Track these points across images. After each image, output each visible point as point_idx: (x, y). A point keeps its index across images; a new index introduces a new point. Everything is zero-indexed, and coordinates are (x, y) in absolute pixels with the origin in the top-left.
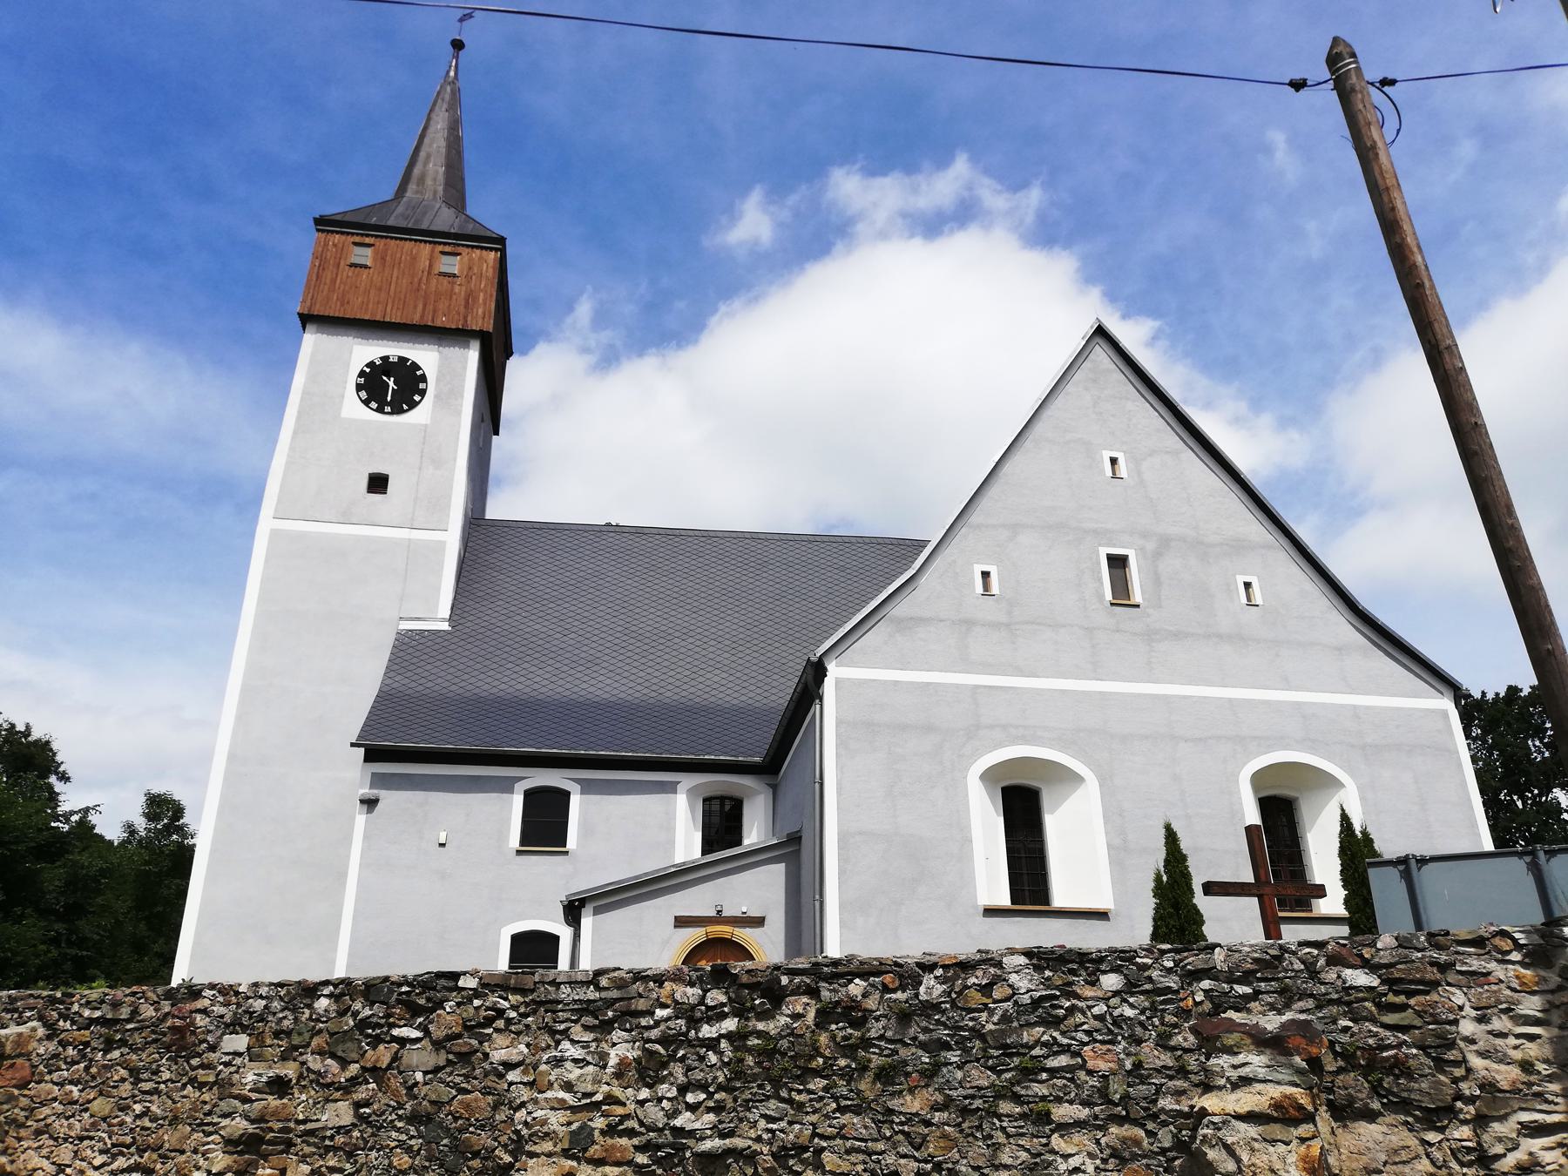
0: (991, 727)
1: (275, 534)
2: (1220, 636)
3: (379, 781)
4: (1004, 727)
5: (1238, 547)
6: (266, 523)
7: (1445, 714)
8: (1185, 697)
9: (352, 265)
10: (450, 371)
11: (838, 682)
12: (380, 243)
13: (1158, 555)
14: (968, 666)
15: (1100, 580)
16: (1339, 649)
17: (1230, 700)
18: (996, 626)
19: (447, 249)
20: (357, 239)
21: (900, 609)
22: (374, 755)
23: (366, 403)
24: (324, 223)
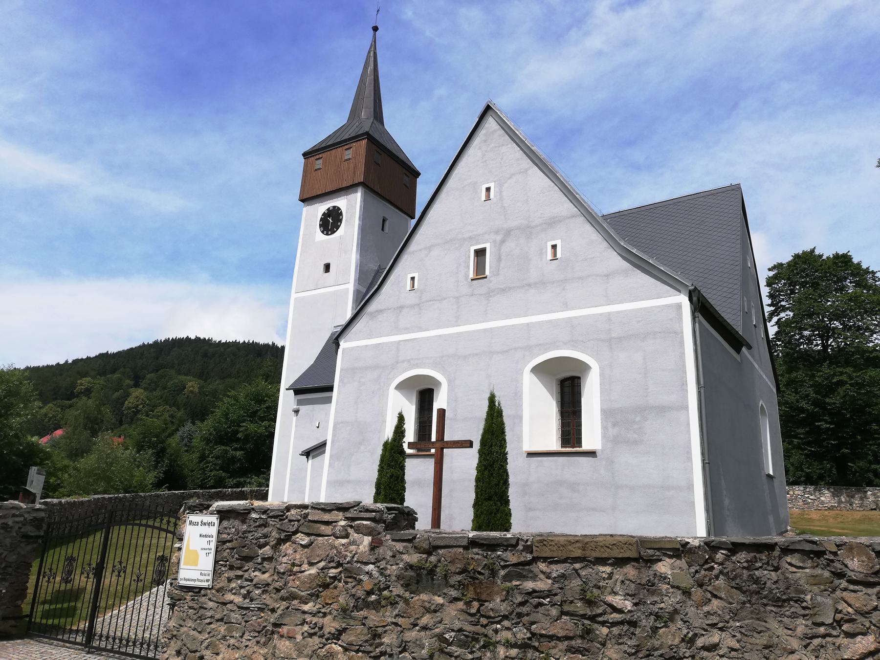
0: (403, 361)
1: (296, 299)
2: (529, 285)
3: (300, 403)
4: (409, 361)
5: (552, 223)
6: (294, 296)
7: (679, 306)
8: (502, 327)
10: (351, 205)
11: (344, 349)
12: (324, 155)
13: (503, 241)
14: (398, 330)
15: (468, 267)
16: (607, 276)
18: (412, 306)
19: (347, 147)
20: (317, 157)
22: (297, 392)
23: (323, 232)
24: (306, 155)
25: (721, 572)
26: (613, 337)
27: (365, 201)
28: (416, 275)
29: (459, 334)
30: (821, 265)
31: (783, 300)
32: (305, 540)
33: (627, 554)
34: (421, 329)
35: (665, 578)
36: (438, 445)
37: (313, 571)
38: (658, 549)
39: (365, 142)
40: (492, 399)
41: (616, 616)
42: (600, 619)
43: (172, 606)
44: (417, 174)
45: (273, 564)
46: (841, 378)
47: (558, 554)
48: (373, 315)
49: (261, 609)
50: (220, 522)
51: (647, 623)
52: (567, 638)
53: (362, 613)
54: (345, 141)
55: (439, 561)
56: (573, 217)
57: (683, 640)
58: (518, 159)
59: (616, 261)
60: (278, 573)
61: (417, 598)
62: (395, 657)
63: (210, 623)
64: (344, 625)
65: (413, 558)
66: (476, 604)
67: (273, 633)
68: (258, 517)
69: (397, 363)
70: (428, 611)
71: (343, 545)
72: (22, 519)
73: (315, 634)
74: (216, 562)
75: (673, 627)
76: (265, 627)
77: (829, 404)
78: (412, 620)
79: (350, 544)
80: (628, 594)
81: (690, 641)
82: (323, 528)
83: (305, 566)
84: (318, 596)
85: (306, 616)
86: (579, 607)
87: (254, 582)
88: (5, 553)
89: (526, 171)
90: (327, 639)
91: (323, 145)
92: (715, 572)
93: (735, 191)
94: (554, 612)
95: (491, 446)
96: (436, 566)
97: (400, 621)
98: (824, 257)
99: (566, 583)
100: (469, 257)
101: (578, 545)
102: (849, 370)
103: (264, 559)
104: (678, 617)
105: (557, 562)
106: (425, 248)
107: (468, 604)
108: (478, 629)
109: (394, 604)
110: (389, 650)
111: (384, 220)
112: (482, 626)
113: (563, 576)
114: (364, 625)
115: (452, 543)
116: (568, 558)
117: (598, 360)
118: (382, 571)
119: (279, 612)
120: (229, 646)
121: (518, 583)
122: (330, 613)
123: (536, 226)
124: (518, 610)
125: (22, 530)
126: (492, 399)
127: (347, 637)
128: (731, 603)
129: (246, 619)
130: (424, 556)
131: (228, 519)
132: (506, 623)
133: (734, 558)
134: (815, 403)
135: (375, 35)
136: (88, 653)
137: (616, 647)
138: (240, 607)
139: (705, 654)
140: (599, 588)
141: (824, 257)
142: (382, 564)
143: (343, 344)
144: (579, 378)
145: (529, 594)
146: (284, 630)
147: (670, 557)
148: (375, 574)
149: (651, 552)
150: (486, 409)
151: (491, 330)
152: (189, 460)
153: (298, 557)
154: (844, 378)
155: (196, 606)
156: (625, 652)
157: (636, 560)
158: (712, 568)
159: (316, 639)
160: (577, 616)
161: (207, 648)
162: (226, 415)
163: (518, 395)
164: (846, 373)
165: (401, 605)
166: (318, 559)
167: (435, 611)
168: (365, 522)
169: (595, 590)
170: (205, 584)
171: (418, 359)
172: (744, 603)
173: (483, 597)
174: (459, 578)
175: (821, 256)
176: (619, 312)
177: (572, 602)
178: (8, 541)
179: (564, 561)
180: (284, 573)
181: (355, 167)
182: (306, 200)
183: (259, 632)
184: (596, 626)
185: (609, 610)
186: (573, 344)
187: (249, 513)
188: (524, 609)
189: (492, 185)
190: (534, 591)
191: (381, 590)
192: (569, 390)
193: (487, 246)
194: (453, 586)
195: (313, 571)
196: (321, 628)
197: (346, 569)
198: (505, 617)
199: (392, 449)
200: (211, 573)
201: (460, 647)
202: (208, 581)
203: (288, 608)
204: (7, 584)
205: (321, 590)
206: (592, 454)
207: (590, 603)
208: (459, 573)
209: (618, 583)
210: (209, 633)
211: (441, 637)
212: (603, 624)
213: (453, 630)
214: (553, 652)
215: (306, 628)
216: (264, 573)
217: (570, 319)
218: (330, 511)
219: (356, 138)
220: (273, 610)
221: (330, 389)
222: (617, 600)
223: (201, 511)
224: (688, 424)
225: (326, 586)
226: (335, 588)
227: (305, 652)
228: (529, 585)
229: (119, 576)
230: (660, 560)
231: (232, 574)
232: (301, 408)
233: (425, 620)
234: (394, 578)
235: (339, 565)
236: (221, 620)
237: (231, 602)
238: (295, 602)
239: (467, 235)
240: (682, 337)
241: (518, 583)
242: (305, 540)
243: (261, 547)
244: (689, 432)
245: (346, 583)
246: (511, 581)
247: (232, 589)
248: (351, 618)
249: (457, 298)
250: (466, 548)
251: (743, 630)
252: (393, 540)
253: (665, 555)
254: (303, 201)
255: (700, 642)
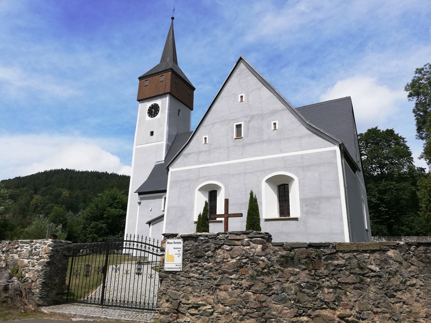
0: (202, 178)
2: (263, 141)
3: (141, 199)
4: (205, 177)
5: (273, 113)
6: (135, 147)
7: (335, 151)
8: (251, 161)
9: (146, 86)
10: (164, 103)
11: (171, 172)
13: (250, 121)
15: (233, 133)
16: (301, 137)
17: (263, 160)
18: (206, 151)
20: (146, 79)
21: (185, 152)
22: (140, 194)
23: (149, 116)
24: (140, 78)
25: (414, 255)
26: (304, 165)
27: (170, 101)
28: (207, 137)
29: (229, 164)
30: (381, 135)
31: (363, 151)
32: (228, 248)
33: (376, 248)
34: (211, 162)
35: (391, 257)
36: (226, 216)
37: (234, 261)
38: (388, 246)
39: (170, 73)
40: (251, 194)
41: (373, 274)
42: (367, 275)
43: (161, 281)
44: (194, 89)
45: (214, 259)
46: (390, 187)
47: (346, 249)
48: (186, 156)
49: (209, 279)
50: (184, 242)
51: (386, 276)
52: (354, 283)
53: (262, 277)
54: (160, 72)
55: (295, 254)
56: (283, 110)
57: (401, 283)
58: (256, 83)
59: (304, 130)
60: (216, 263)
61: (287, 269)
62: (280, 294)
63: (183, 287)
64: (252, 283)
65: (284, 253)
66: (313, 271)
67: (216, 289)
68: (203, 238)
69: (199, 178)
70: (293, 275)
71: (248, 249)
72: (63, 247)
73: (238, 288)
74: (183, 260)
75: (396, 278)
76: (212, 286)
77: (385, 199)
78: (286, 279)
79: (251, 248)
80: (377, 265)
81: (404, 283)
82: (236, 242)
83: (229, 259)
84: (237, 271)
85: (233, 280)
86: (357, 270)
87: (204, 267)
88: (57, 263)
89: (259, 89)
90: (244, 290)
91: (149, 74)
92: (411, 255)
93: (349, 99)
94: (347, 273)
95: (253, 216)
96: (294, 256)
97: (280, 279)
98: (381, 131)
99: (351, 261)
100: (233, 128)
101: (355, 245)
102: (394, 183)
103: (208, 257)
104: (398, 274)
105: (346, 253)
106: (211, 124)
107: (310, 271)
108: (315, 281)
109: (276, 272)
110: (276, 292)
111: (179, 111)
112: (317, 280)
113: (350, 258)
114: (263, 282)
115: (301, 246)
116: (351, 251)
117: (297, 176)
118: (269, 259)
119: (219, 279)
120: (194, 296)
121: (331, 262)
122: (245, 278)
123: (266, 114)
124: (332, 273)
125: (63, 253)
126: (251, 194)
127: (254, 288)
128: (419, 267)
129: (201, 283)
130: (288, 252)
131: (188, 240)
132: (327, 278)
133: (418, 249)
134: (378, 199)
135: (172, 21)
136: (103, 308)
137: (374, 286)
138: (197, 279)
139: (411, 288)
140: (365, 262)
141: (381, 131)
142: (269, 256)
143: (171, 169)
144: (288, 185)
145: (336, 266)
146: (222, 287)
147: (393, 249)
148: (266, 260)
149: (385, 247)
150: (249, 199)
151: (245, 162)
152: (78, 229)
153: (226, 255)
154: (392, 186)
155: (175, 280)
156: (378, 288)
157: (379, 250)
158: (410, 253)
159: (239, 290)
160: (356, 274)
161: (183, 298)
162: (97, 206)
163: (260, 192)
164: (393, 184)
165: (280, 273)
166: (236, 255)
167: (296, 275)
168: (258, 239)
169: (363, 263)
170: (179, 270)
171: (210, 176)
172: (424, 267)
173: (316, 268)
174: (305, 260)
175: (380, 130)
176: (307, 154)
177: (354, 269)
178: (58, 258)
179: (350, 252)
180: (219, 263)
181: (166, 85)
182: (141, 100)
183: (209, 289)
184: (364, 278)
185: (370, 271)
186: (285, 168)
187: (198, 237)
188: (334, 272)
189: (243, 95)
190: (338, 265)
191: (269, 267)
192: (283, 190)
193: (242, 123)
194: (303, 264)
195: (234, 261)
196: (241, 285)
197: (251, 259)
198: (327, 276)
199: (203, 218)
200: (181, 265)
201: (308, 289)
202: (180, 268)
203: (223, 277)
204: (58, 278)
205: (239, 268)
206: (296, 219)
207: (362, 268)
208: (305, 258)
209: (372, 260)
210: (183, 291)
211: (299, 285)
212: (368, 277)
213: (305, 282)
214: (348, 289)
215: (233, 285)
216: (209, 263)
217: (284, 157)
218: (239, 235)
219: (166, 71)
220: (215, 279)
221: (165, 191)
222: (373, 267)
223: (173, 238)
224: (341, 205)
225: (241, 267)
226: (246, 267)
227: (234, 296)
228: (336, 262)
229: (116, 272)
230: (389, 250)
231: (192, 264)
232: (142, 201)
233: (292, 278)
234: (275, 262)
235: (247, 257)
236: (189, 285)
237: (193, 277)
238: (226, 275)
239: (232, 118)
240: (337, 165)
241: (331, 262)
242: (228, 248)
243: (206, 251)
244: (341, 208)
245: (252, 265)
246: (327, 261)
247: (193, 271)
248: (256, 279)
249: (228, 147)
250: (307, 248)
251: (425, 278)
252: (273, 246)
253: (391, 248)
254: (139, 101)
255: (408, 283)
